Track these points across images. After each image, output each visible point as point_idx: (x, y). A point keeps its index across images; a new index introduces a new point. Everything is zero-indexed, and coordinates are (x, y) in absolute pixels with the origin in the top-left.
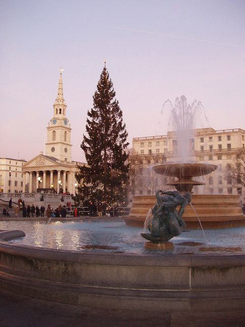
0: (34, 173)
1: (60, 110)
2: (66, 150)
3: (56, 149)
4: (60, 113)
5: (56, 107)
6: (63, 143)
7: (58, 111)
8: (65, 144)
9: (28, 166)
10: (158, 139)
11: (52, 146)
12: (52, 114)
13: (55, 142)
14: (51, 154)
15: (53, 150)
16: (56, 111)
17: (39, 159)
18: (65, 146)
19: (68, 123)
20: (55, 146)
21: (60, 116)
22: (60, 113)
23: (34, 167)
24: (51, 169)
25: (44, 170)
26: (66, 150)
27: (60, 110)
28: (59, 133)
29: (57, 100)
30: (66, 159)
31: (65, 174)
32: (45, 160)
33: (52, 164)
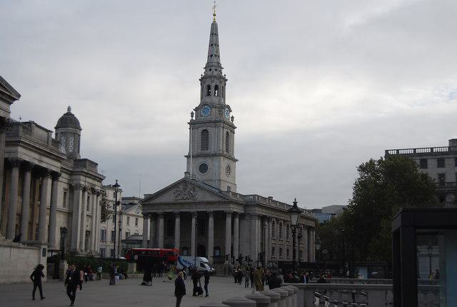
0: (170, 219)
1: (216, 88)
3: (210, 166)
5: (208, 82)
9: (152, 202)
10: (442, 153)
11: (201, 161)
13: (207, 152)
14: (200, 177)
15: (203, 168)
17: (181, 187)
19: (231, 114)
20: (208, 161)
24: (211, 209)
25: (193, 210)
26: (229, 169)
27: (216, 88)
28: (216, 135)
30: (229, 187)
31: (237, 220)
32: (197, 189)
33: (209, 198)
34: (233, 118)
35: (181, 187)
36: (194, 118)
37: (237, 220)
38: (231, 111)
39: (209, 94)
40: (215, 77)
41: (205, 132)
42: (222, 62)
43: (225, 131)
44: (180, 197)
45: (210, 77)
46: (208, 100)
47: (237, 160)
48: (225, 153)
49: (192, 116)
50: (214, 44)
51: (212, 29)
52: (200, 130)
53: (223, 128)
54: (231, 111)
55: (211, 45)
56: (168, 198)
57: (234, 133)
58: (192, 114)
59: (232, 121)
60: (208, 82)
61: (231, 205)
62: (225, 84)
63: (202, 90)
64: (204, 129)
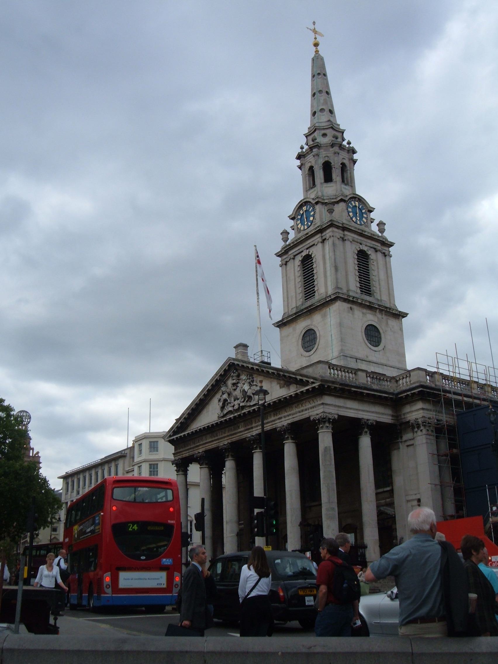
1: (327, 167)
2: (373, 335)
4: (328, 178)
5: (310, 160)
7: (319, 175)
8: (371, 307)
11: (302, 325)
12: (290, 186)
15: (309, 339)
18: (371, 318)
20: (316, 321)
21: (330, 190)
22: (328, 178)
23: (210, 430)
24: (282, 421)
26: (373, 335)
31: (365, 443)
34: (381, 225)
35: (230, 382)
37: (365, 443)
40: (318, 146)
44: (229, 408)
46: (312, 195)
47: (404, 315)
49: (285, 240)
50: (321, 92)
53: (343, 240)
56: (211, 416)
58: (285, 233)
59: (382, 231)
60: (310, 160)
61: (328, 399)
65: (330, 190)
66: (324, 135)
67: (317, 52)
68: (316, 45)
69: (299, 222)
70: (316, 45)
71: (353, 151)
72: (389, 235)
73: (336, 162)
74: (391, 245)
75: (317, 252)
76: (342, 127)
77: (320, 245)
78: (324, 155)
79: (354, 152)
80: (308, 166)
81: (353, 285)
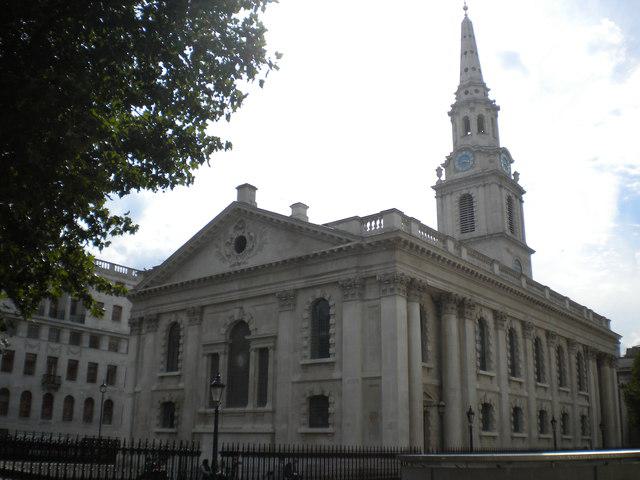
4: (481, 128)
6: (508, 239)
16: (461, 130)
22: (481, 128)
29: (463, 90)
34: (516, 174)
36: (443, 178)
38: (512, 161)
39: (467, 128)
40: (475, 101)
41: (467, 202)
42: (486, 79)
43: (505, 193)
45: (468, 102)
47: (533, 252)
48: (509, 233)
49: (439, 175)
50: (469, 50)
51: (463, 28)
52: (456, 197)
53: (500, 186)
54: (512, 161)
55: (464, 53)
57: (522, 201)
58: (439, 171)
60: (466, 112)
62: (496, 116)
63: (455, 130)
64: (465, 192)
65: (482, 141)
66: (477, 91)
67: (466, 15)
68: (465, 9)
69: (456, 163)
70: (465, 9)
71: (498, 108)
72: (521, 183)
73: (487, 116)
74: (524, 192)
75: (479, 195)
76: (488, 86)
77: (481, 189)
78: (481, 110)
79: (498, 108)
80: (462, 116)
81: (507, 226)
